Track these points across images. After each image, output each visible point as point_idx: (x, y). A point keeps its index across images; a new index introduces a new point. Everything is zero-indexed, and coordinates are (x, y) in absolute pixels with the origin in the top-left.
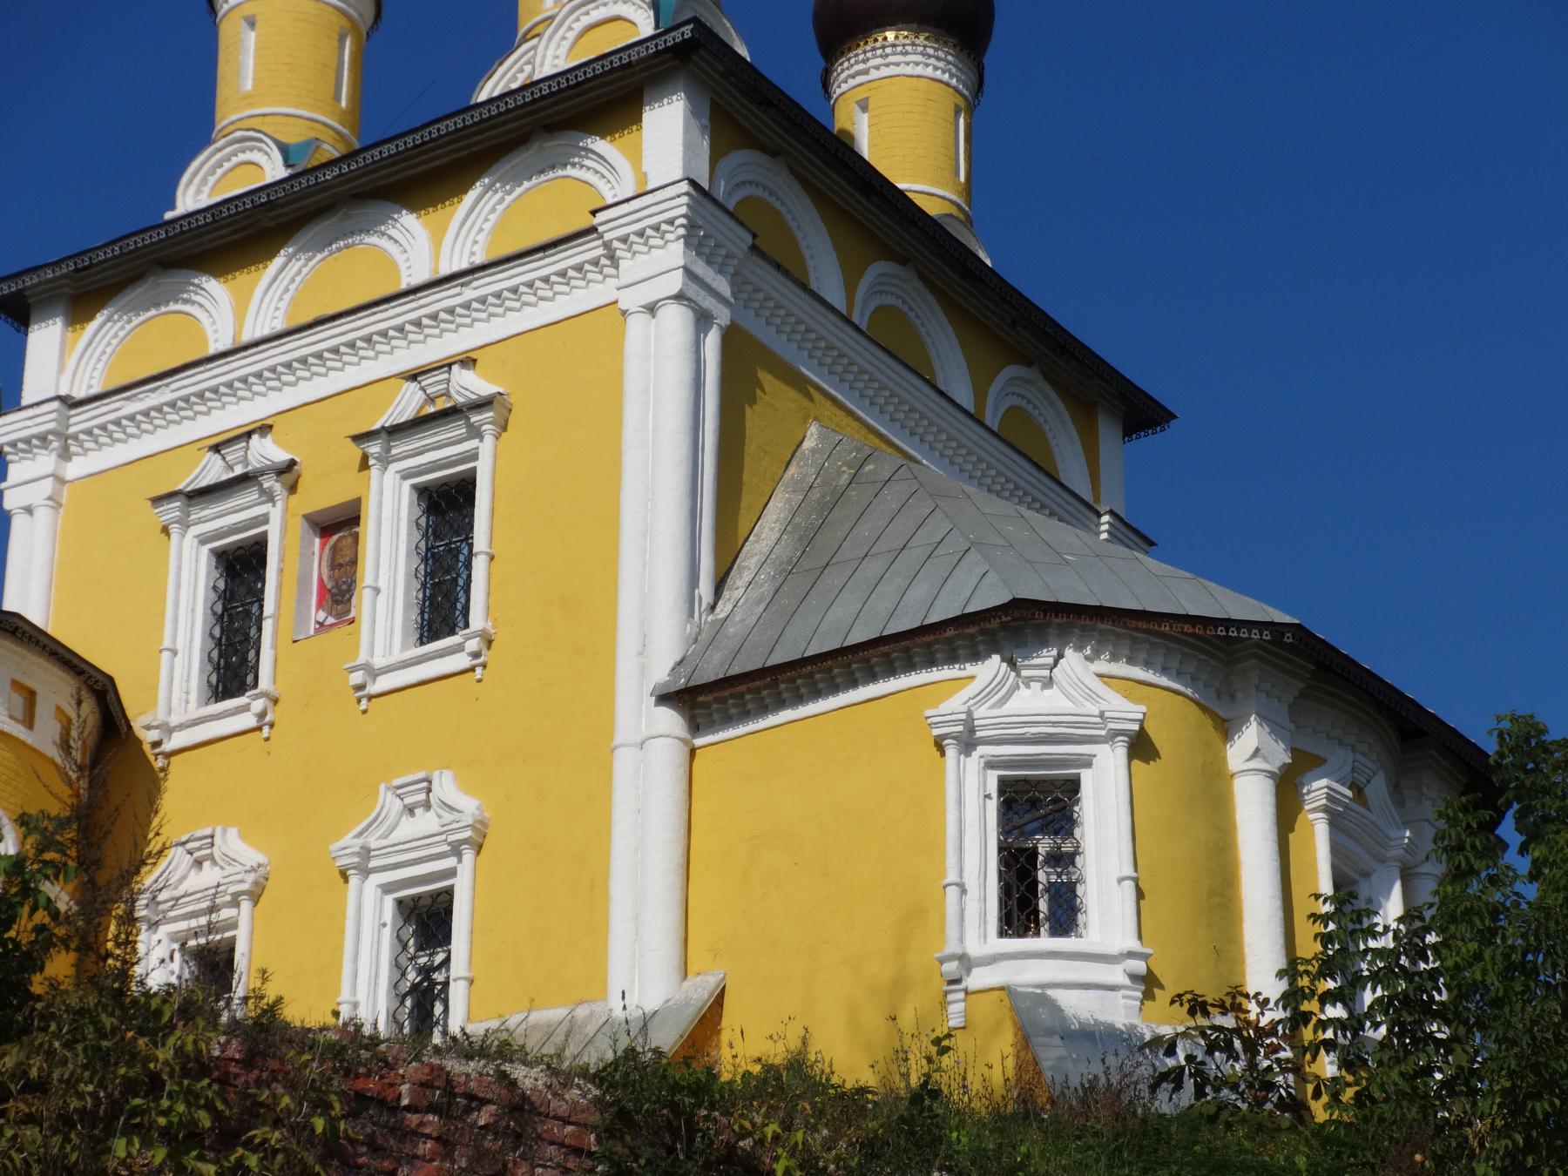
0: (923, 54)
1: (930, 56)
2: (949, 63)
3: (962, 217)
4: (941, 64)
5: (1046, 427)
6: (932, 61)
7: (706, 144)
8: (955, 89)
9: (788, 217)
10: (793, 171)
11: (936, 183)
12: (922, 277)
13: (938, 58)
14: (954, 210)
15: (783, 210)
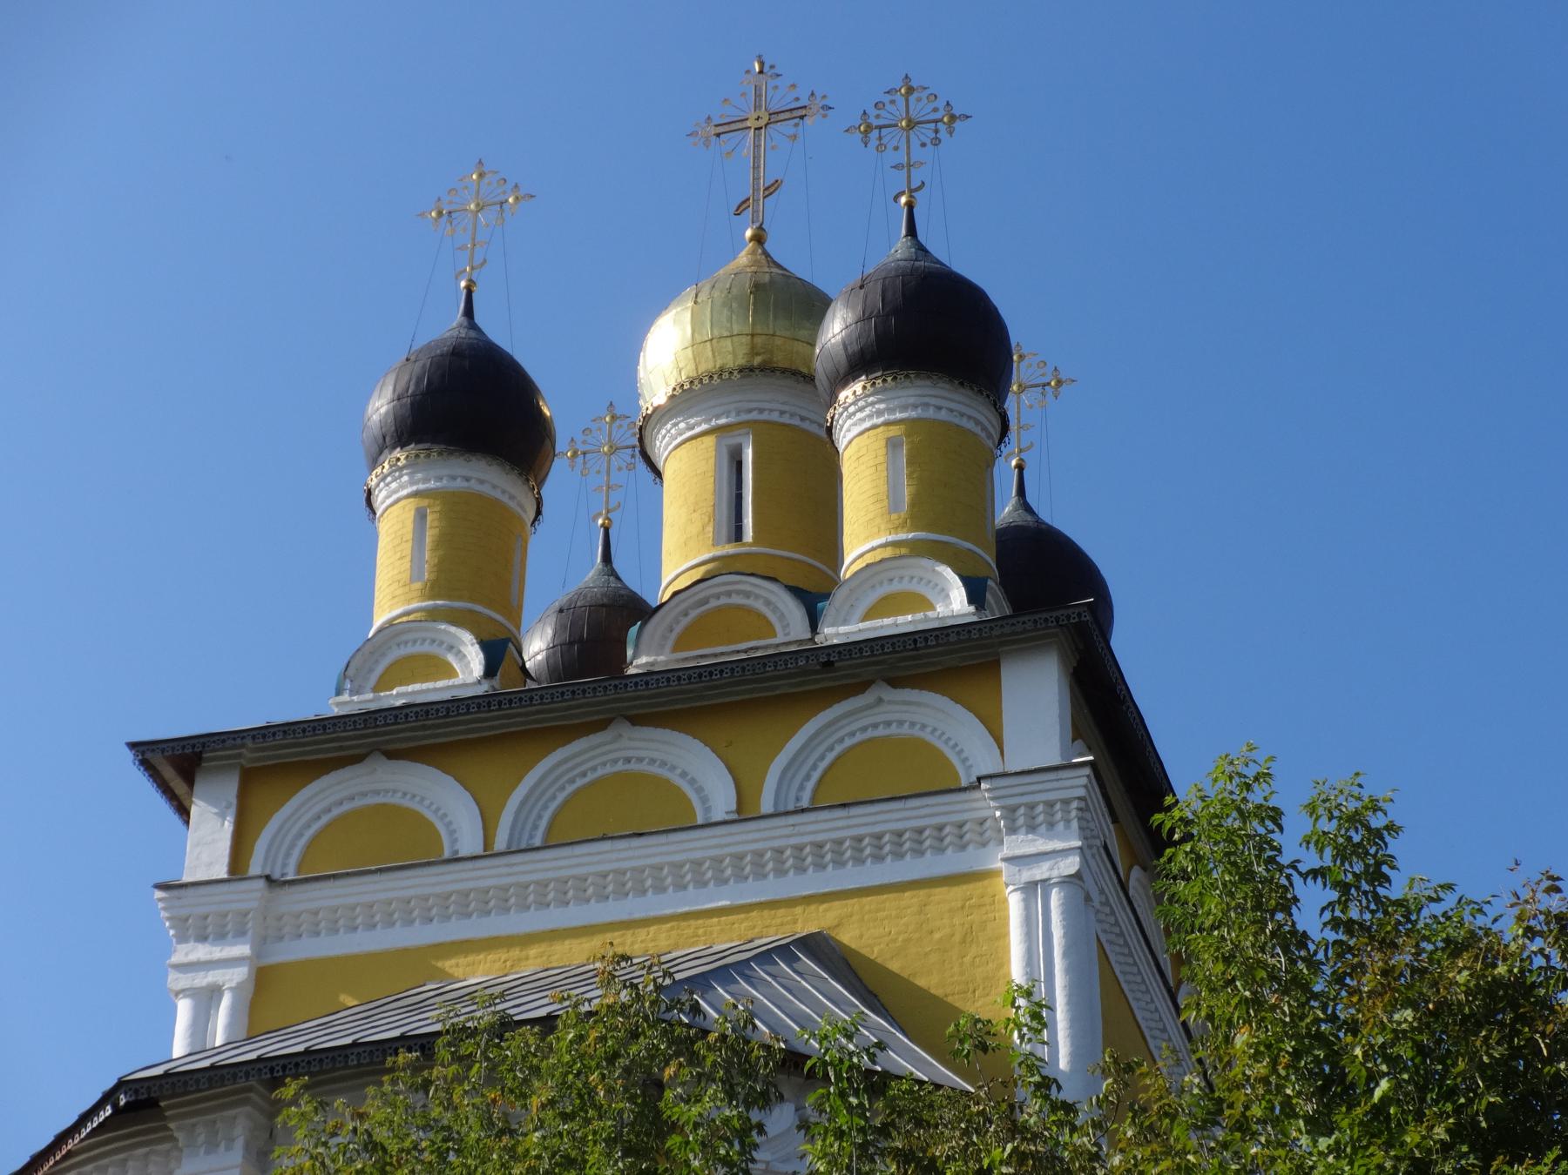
0: (849, 417)
1: (854, 414)
2: (873, 404)
3: (904, 551)
4: (867, 411)
5: (926, 735)
6: (859, 415)
7: (228, 826)
8: (887, 424)
9: (406, 803)
10: (392, 755)
11: (867, 539)
12: (636, 721)
13: (861, 409)
14: (888, 553)
15: (396, 800)
